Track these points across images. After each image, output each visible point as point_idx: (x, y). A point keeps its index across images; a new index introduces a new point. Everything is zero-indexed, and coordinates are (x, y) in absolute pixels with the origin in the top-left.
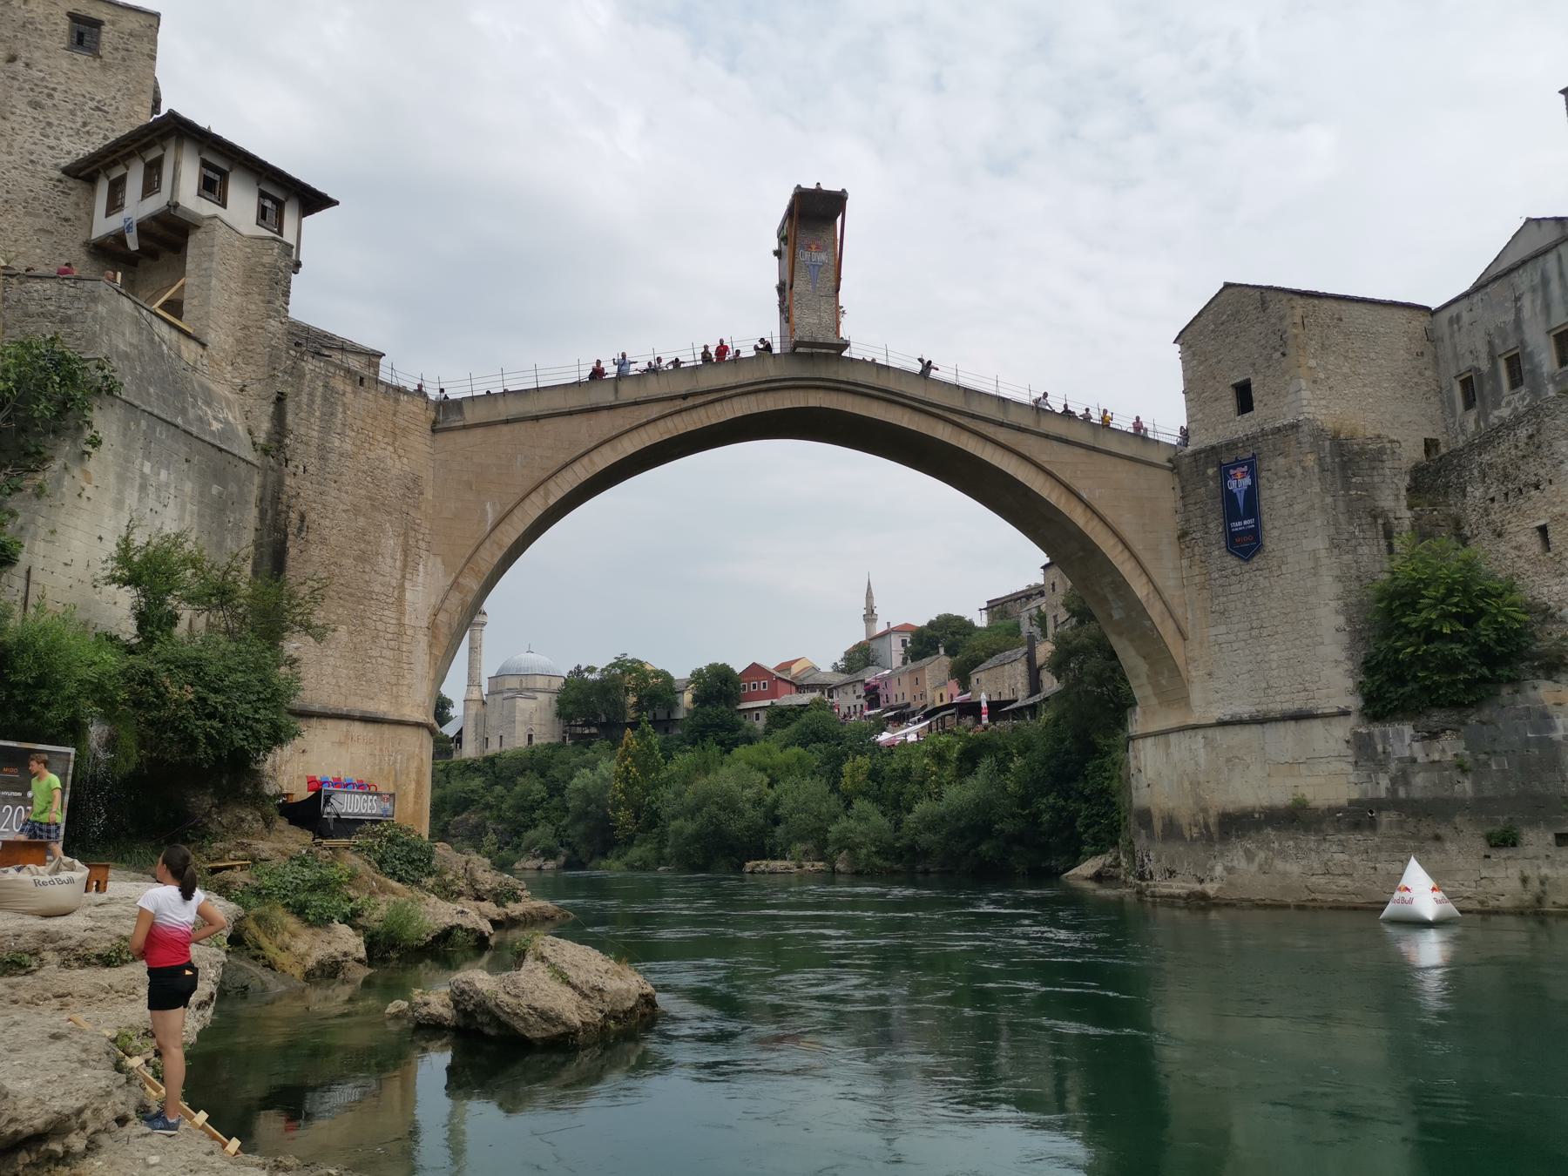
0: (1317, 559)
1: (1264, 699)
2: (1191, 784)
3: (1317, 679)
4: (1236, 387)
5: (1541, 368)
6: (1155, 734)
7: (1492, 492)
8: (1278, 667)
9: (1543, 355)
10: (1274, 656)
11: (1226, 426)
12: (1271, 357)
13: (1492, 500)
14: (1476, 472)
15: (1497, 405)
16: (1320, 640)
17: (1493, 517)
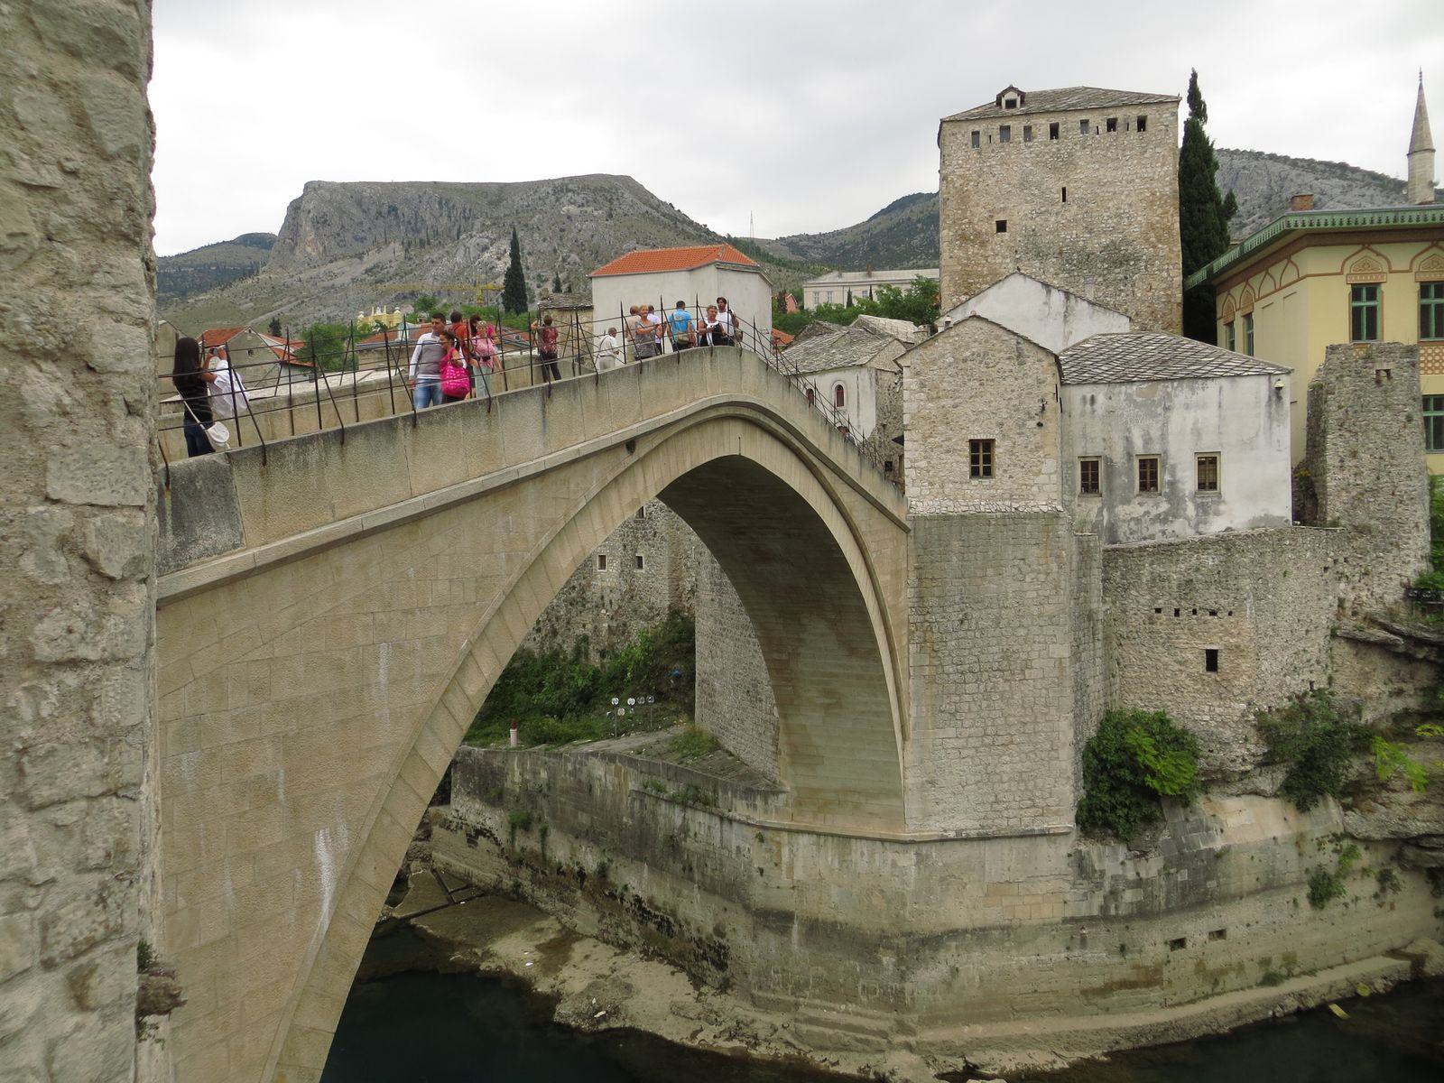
0: (1062, 669)
1: (991, 815)
2: (888, 902)
3: (1048, 795)
4: (974, 445)
5: (1183, 484)
6: (819, 835)
7: (1160, 603)
8: (1010, 780)
9: (1187, 473)
10: (1007, 768)
11: (958, 486)
12: (1024, 425)
13: (1158, 611)
14: (1144, 580)
15: (1127, 501)
16: (1056, 755)
17: (1157, 627)
